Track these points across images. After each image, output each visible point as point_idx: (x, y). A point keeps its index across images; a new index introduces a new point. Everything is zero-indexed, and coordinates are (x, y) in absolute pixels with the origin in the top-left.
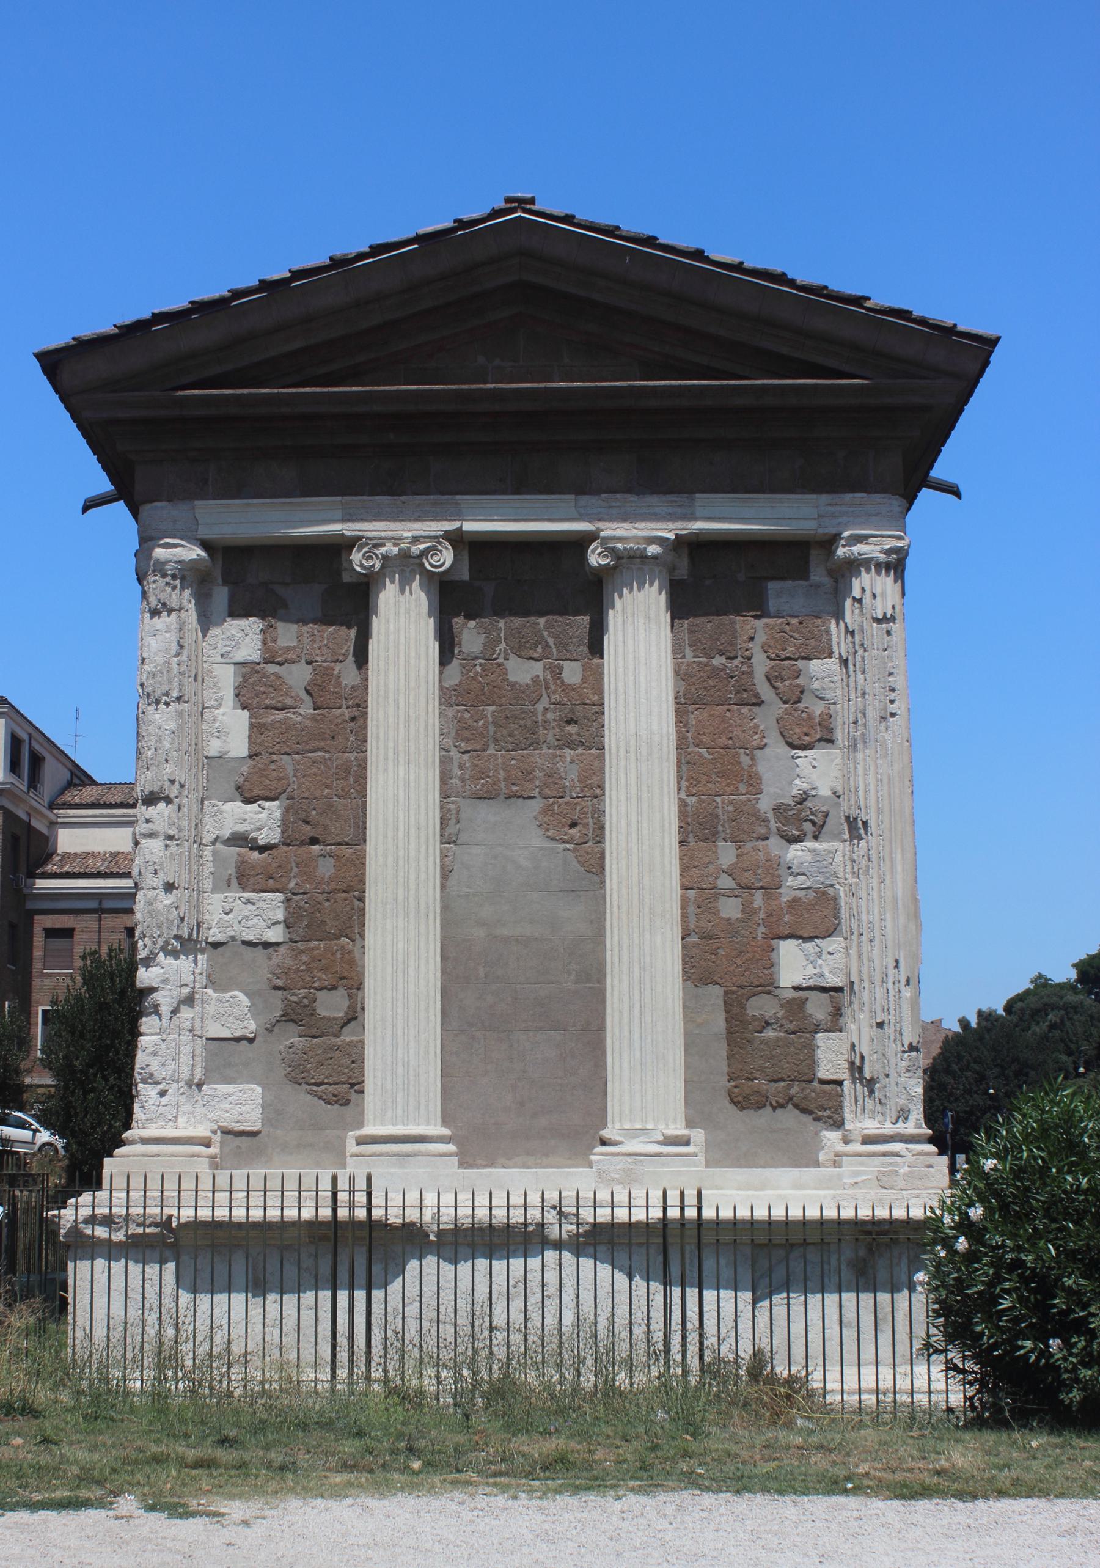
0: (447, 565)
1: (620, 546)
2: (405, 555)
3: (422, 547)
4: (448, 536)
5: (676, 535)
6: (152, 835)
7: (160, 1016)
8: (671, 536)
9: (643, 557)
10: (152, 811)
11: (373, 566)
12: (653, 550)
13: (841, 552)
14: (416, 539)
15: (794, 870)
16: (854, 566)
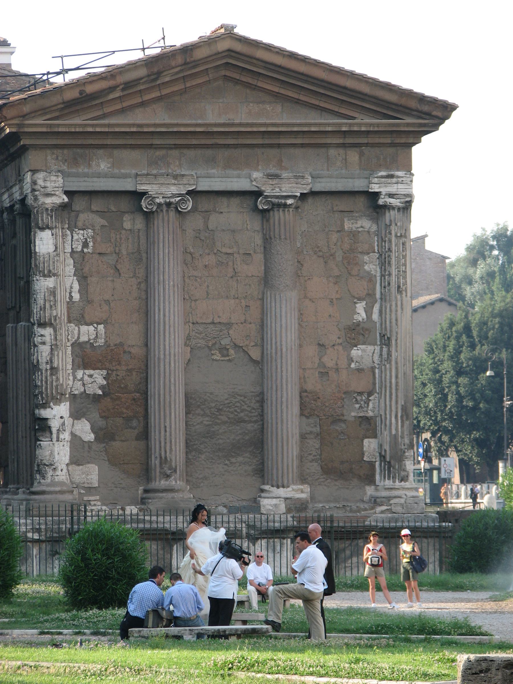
0: (189, 208)
1: (274, 200)
2: (168, 205)
3: (178, 199)
4: (189, 193)
5: (301, 194)
6: (44, 343)
7: (51, 433)
8: (298, 194)
9: (285, 205)
10: (41, 331)
11: (152, 208)
12: (290, 202)
13: (381, 202)
14: (174, 196)
15: (355, 360)
16: (386, 207)
